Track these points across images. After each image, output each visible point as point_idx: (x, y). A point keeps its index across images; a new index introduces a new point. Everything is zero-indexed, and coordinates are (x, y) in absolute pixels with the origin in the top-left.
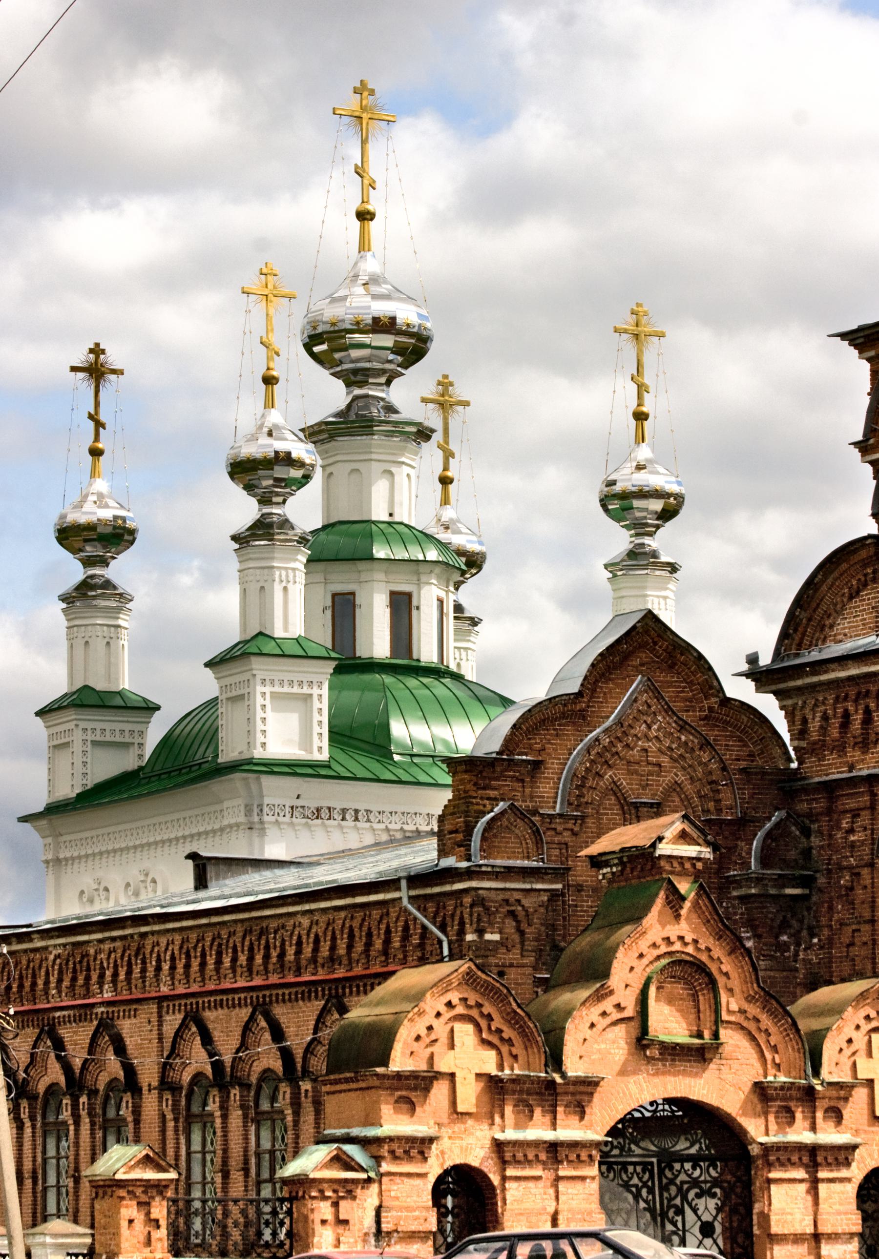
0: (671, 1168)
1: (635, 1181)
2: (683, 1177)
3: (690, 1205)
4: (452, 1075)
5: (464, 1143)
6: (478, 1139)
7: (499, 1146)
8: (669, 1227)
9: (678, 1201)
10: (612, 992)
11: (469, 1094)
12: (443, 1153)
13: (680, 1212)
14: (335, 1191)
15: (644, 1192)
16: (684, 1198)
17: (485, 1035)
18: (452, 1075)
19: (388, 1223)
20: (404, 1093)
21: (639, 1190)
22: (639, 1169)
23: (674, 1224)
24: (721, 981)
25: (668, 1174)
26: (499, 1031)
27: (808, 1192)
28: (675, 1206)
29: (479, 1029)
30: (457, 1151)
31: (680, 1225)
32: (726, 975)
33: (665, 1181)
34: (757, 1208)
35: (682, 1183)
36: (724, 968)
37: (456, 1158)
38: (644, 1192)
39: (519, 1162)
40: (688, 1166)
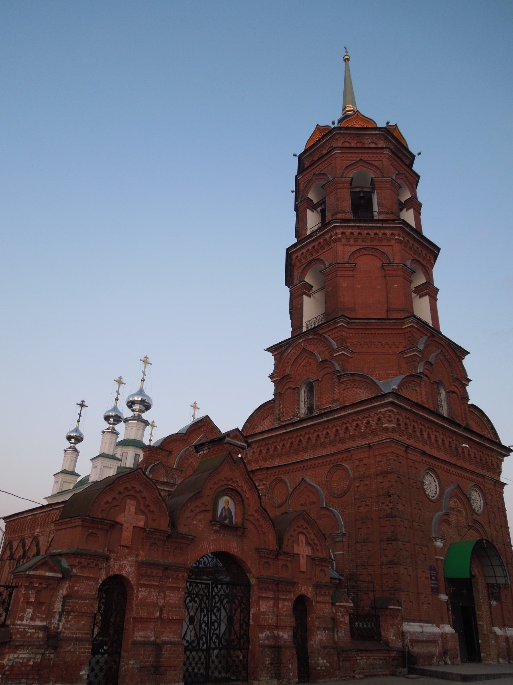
0: (217, 587)
1: (201, 592)
2: (222, 592)
3: (224, 606)
4: (122, 525)
5: (122, 563)
6: (129, 561)
7: (140, 565)
8: (214, 618)
9: (218, 605)
10: (202, 497)
11: (127, 535)
12: (109, 567)
13: (219, 610)
14: (40, 584)
15: (205, 598)
16: (222, 603)
17: (142, 507)
18: (122, 525)
19: (69, 606)
20: (94, 531)
21: (202, 597)
22: (204, 586)
23: (216, 616)
24: (246, 501)
25: (216, 590)
26: (148, 506)
27: (274, 604)
28: (217, 607)
29: (139, 503)
30: (117, 567)
31: (219, 618)
32: (247, 498)
33: (214, 594)
34: (252, 611)
35: (222, 595)
36: (248, 496)
37: (115, 570)
38: (205, 598)
39: (148, 576)
40: (224, 587)
